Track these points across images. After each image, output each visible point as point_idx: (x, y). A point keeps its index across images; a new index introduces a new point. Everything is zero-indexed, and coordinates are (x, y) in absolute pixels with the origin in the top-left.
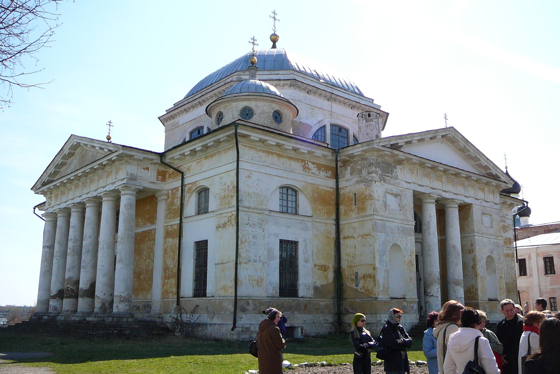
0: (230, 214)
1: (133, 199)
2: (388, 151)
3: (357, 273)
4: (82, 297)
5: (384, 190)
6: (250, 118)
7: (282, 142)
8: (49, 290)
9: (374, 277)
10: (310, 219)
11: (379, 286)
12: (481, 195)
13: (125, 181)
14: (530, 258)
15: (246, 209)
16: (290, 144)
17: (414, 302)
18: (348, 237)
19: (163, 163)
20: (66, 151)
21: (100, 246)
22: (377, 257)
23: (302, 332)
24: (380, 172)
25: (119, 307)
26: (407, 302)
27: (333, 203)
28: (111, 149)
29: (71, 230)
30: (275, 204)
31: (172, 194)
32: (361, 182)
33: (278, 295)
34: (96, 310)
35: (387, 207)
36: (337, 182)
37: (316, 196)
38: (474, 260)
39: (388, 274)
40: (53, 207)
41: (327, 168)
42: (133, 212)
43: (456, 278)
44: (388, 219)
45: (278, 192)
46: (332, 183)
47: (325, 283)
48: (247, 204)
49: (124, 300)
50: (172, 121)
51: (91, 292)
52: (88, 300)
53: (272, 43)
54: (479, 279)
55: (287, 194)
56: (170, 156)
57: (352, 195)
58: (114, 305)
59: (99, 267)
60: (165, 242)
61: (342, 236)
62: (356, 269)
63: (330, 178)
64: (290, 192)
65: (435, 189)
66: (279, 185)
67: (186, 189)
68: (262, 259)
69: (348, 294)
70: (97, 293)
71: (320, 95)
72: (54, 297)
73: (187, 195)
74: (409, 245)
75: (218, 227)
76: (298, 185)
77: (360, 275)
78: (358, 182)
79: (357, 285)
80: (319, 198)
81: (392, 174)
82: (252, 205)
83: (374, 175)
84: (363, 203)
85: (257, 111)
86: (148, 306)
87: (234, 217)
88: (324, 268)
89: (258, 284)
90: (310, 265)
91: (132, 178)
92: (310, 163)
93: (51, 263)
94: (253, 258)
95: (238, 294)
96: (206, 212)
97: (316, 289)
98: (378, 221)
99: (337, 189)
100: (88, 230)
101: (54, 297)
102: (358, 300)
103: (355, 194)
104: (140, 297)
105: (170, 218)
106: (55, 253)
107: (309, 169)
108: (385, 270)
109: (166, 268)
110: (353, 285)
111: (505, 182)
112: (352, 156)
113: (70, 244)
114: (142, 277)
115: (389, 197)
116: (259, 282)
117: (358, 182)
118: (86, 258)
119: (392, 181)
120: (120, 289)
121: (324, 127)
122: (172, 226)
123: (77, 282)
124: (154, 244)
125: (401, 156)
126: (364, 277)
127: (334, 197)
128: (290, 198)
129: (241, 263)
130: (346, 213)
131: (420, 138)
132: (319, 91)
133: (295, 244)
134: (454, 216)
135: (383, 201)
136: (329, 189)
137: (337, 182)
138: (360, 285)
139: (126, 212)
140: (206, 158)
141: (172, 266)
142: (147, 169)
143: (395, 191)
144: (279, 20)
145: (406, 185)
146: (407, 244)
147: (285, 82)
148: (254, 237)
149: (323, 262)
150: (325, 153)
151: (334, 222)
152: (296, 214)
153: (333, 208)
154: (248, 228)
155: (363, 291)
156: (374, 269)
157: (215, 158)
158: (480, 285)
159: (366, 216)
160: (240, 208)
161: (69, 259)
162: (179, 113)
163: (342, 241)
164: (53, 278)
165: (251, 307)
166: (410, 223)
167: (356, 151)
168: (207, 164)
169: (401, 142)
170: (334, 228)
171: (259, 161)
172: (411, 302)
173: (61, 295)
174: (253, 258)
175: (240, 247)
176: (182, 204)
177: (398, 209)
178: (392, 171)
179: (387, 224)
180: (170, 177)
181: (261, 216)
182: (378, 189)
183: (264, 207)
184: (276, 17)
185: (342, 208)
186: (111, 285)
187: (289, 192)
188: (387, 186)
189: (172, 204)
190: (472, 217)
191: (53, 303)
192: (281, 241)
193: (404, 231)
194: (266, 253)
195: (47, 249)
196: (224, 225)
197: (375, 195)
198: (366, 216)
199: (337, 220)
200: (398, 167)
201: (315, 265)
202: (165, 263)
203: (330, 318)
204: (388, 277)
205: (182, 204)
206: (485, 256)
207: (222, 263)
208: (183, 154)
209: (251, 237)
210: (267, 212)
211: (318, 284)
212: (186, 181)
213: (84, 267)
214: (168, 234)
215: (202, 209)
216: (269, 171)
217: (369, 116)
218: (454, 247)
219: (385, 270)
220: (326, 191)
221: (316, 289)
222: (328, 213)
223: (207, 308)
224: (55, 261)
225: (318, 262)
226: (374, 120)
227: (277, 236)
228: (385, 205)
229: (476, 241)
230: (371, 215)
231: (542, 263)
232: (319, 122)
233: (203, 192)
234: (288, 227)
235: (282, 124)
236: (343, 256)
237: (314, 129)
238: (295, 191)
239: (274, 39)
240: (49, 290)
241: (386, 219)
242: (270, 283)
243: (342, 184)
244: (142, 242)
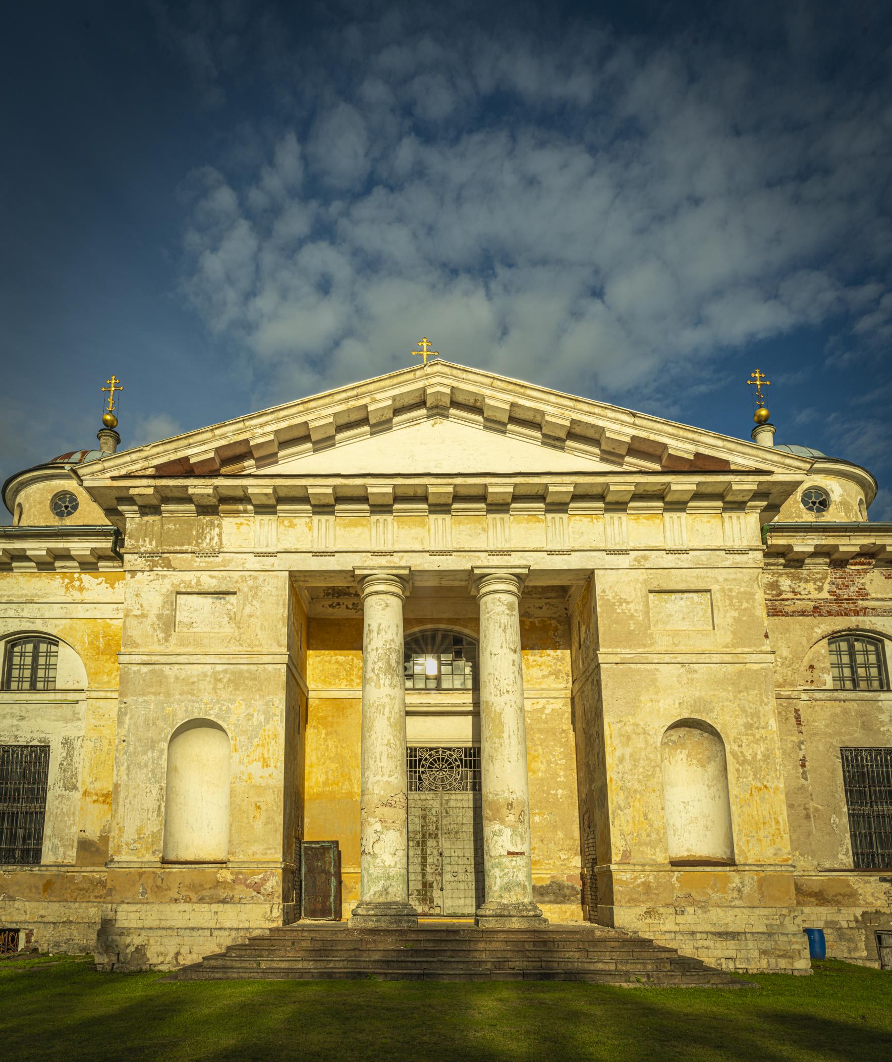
44: (173, 659)
81: (198, 544)
98: (135, 668)
119: (199, 562)
135: (159, 617)
143: (209, 581)
145: (252, 563)
177: (228, 630)
188: (176, 578)
228: (168, 624)
241: (162, 659)
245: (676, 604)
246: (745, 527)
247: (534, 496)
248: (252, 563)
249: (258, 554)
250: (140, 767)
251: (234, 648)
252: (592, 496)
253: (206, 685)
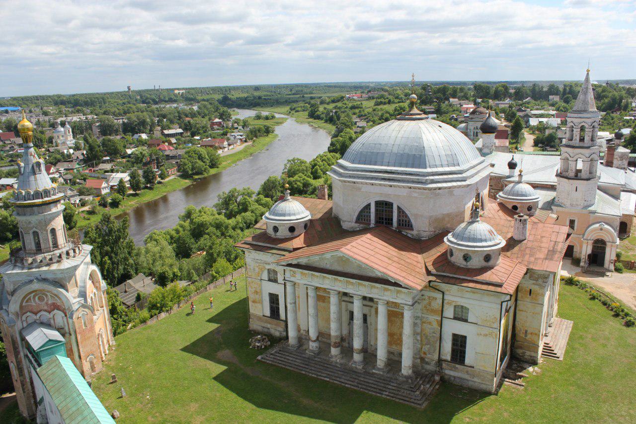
18: (522, 311)
32: (537, 285)
61: (517, 309)
67: (445, 302)
69: (518, 338)
78: (534, 284)
79: (526, 336)
84: (536, 296)
102: (526, 344)
103: (531, 290)
117: (534, 284)
126: (532, 333)
155: (530, 340)
163: (517, 311)
195: (293, 305)
212: (446, 297)
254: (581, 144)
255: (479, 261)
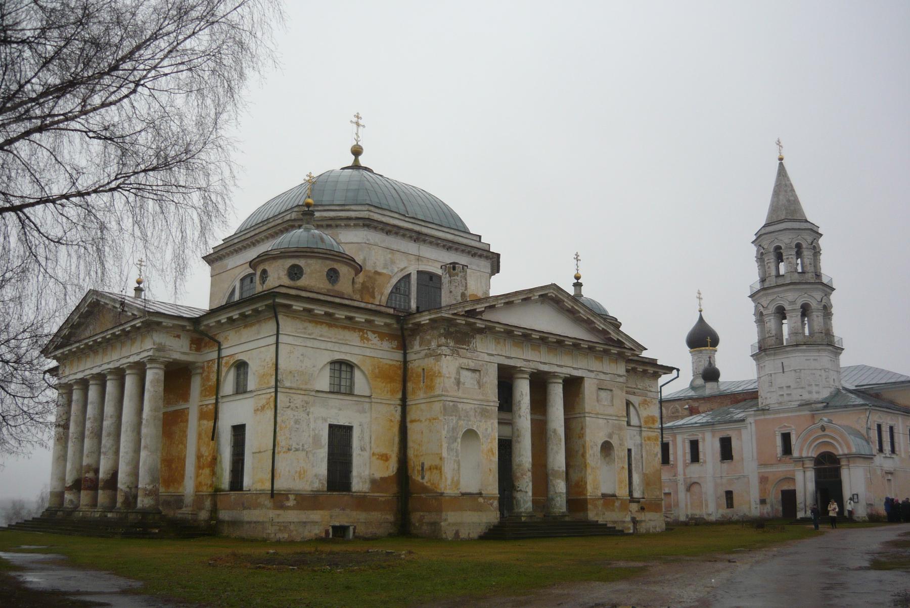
0: (268, 396)
1: (161, 373)
2: (461, 321)
3: (423, 464)
4: (103, 488)
5: (457, 365)
6: (299, 278)
7: (331, 311)
8: (63, 479)
9: (440, 469)
10: (367, 400)
11: (446, 478)
12: (595, 365)
13: (151, 353)
14: (704, 439)
15: (288, 390)
16: (341, 312)
17: (493, 498)
19: (195, 331)
20: (84, 309)
21: (123, 429)
22: (445, 445)
23: (354, 532)
24: (452, 344)
25: (143, 502)
26: (484, 498)
27: (399, 379)
28: (136, 313)
29: (89, 408)
30: (324, 382)
31: (208, 367)
33: (325, 489)
34: (119, 505)
35: (461, 385)
36: (405, 355)
37: (377, 371)
38: (584, 447)
39: (459, 465)
40: (67, 376)
41: (391, 337)
42: (161, 389)
43: (556, 468)
45: (328, 368)
46: (398, 356)
47: (386, 475)
48: (288, 384)
49: (148, 493)
50: (219, 264)
51: (112, 482)
52: (108, 492)
53: (353, 157)
54: (589, 471)
55: (340, 370)
56: (205, 323)
57: (420, 370)
58: (139, 499)
59: (121, 454)
60: (199, 425)
61: (408, 419)
62: (422, 460)
63: (397, 348)
64: (344, 368)
65: (529, 361)
66: (329, 360)
68: (306, 446)
70: (119, 485)
71: (404, 236)
72: (70, 489)
73: (224, 370)
74: (489, 430)
75: (256, 410)
76: (354, 360)
77: (426, 467)
79: (423, 478)
80: (382, 374)
82: (294, 385)
83: (443, 348)
84: (432, 380)
85: (306, 270)
86: (178, 501)
87: (272, 399)
88: (385, 458)
89: (300, 476)
90: (366, 454)
91: (160, 348)
92: (369, 333)
93: (65, 447)
94: (294, 446)
95: (275, 487)
96: (245, 392)
97: (374, 482)
99: (405, 362)
100: (109, 409)
101: (70, 489)
104: (171, 490)
105: (205, 396)
106: (71, 435)
107: (368, 340)
108: (455, 461)
109: (199, 457)
110: (419, 478)
111: (632, 349)
112: (419, 325)
113: (88, 424)
114: (173, 466)
115: (466, 374)
116: (301, 474)
117: (427, 356)
118: (106, 442)
119: (469, 355)
120: (144, 482)
121: (409, 275)
122: (207, 405)
123: (97, 471)
124: (187, 427)
125: (480, 324)
127: (400, 372)
128: (343, 376)
129: (279, 453)
130: (414, 392)
131: (507, 300)
132: (402, 232)
133: (349, 429)
134: (557, 393)
136: (394, 363)
137: (405, 355)
138: (426, 478)
139: (152, 389)
140: (246, 326)
141: (207, 454)
142: (178, 336)
143: (472, 365)
144: (364, 126)
145: (487, 358)
146: (486, 429)
147: (356, 222)
148: (297, 422)
149: (383, 450)
150: (388, 321)
151: (399, 402)
152: (351, 394)
153: (398, 386)
154: (289, 412)
155: (429, 485)
156: (441, 459)
157: (254, 329)
158: (590, 479)
159: (434, 397)
160: (279, 389)
161: (87, 443)
162: (228, 255)
163: (409, 425)
164: (69, 466)
165: (291, 503)
166: (492, 404)
167: (423, 319)
168: (247, 334)
169: (480, 307)
170: (399, 408)
171: (305, 333)
172: (491, 498)
173: (77, 485)
174: (294, 446)
175: (278, 434)
176: (218, 380)
177: (476, 387)
178: (468, 343)
179: (460, 406)
180: (205, 346)
181: (306, 398)
182: (448, 365)
183: (309, 387)
184: (361, 122)
185: (410, 385)
186: (135, 474)
187: (342, 368)
189: (208, 379)
190: (583, 393)
191: (68, 496)
192: (331, 426)
193: (484, 413)
194: (311, 440)
196: (263, 408)
197: (444, 371)
198: (434, 397)
199: (404, 400)
200: (478, 336)
201: (374, 454)
202: (199, 450)
203: (390, 517)
204: (459, 469)
205: (218, 380)
206: (600, 443)
207: (260, 452)
208: (219, 321)
209: (292, 423)
210: (313, 393)
211: (378, 475)
212: (224, 353)
213: (105, 454)
214: (203, 416)
215: (241, 389)
216: (317, 344)
217: (454, 268)
218: (555, 431)
219: (455, 461)
220: (390, 365)
221: (374, 482)
222: (393, 392)
223: (243, 504)
224: (70, 444)
225: (377, 451)
226: (460, 274)
227: (325, 420)
228: (458, 383)
229: (587, 423)
230: (439, 396)
231: (717, 445)
232: (402, 270)
233: (241, 366)
234: (340, 410)
235: (339, 284)
236: (410, 444)
237: (394, 281)
238: (350, 366)
239: (357, 152)
240: (63, 479)
242: (316, 475)
243: (411, 357)
244: (172, 424)
245: (603, 394)
246: (621, 369)
247: (576, 347)
248: (487, 358)
249: (489, 354)
250: (452, 450)
251: (481, 397)
252: (591, 349)
253: (472, 413)
254: (780, 281)
255: (279, 278)
